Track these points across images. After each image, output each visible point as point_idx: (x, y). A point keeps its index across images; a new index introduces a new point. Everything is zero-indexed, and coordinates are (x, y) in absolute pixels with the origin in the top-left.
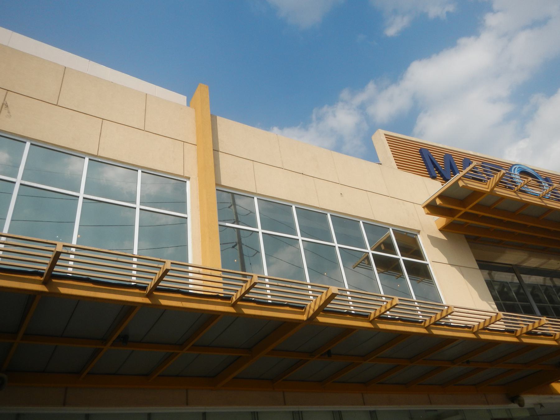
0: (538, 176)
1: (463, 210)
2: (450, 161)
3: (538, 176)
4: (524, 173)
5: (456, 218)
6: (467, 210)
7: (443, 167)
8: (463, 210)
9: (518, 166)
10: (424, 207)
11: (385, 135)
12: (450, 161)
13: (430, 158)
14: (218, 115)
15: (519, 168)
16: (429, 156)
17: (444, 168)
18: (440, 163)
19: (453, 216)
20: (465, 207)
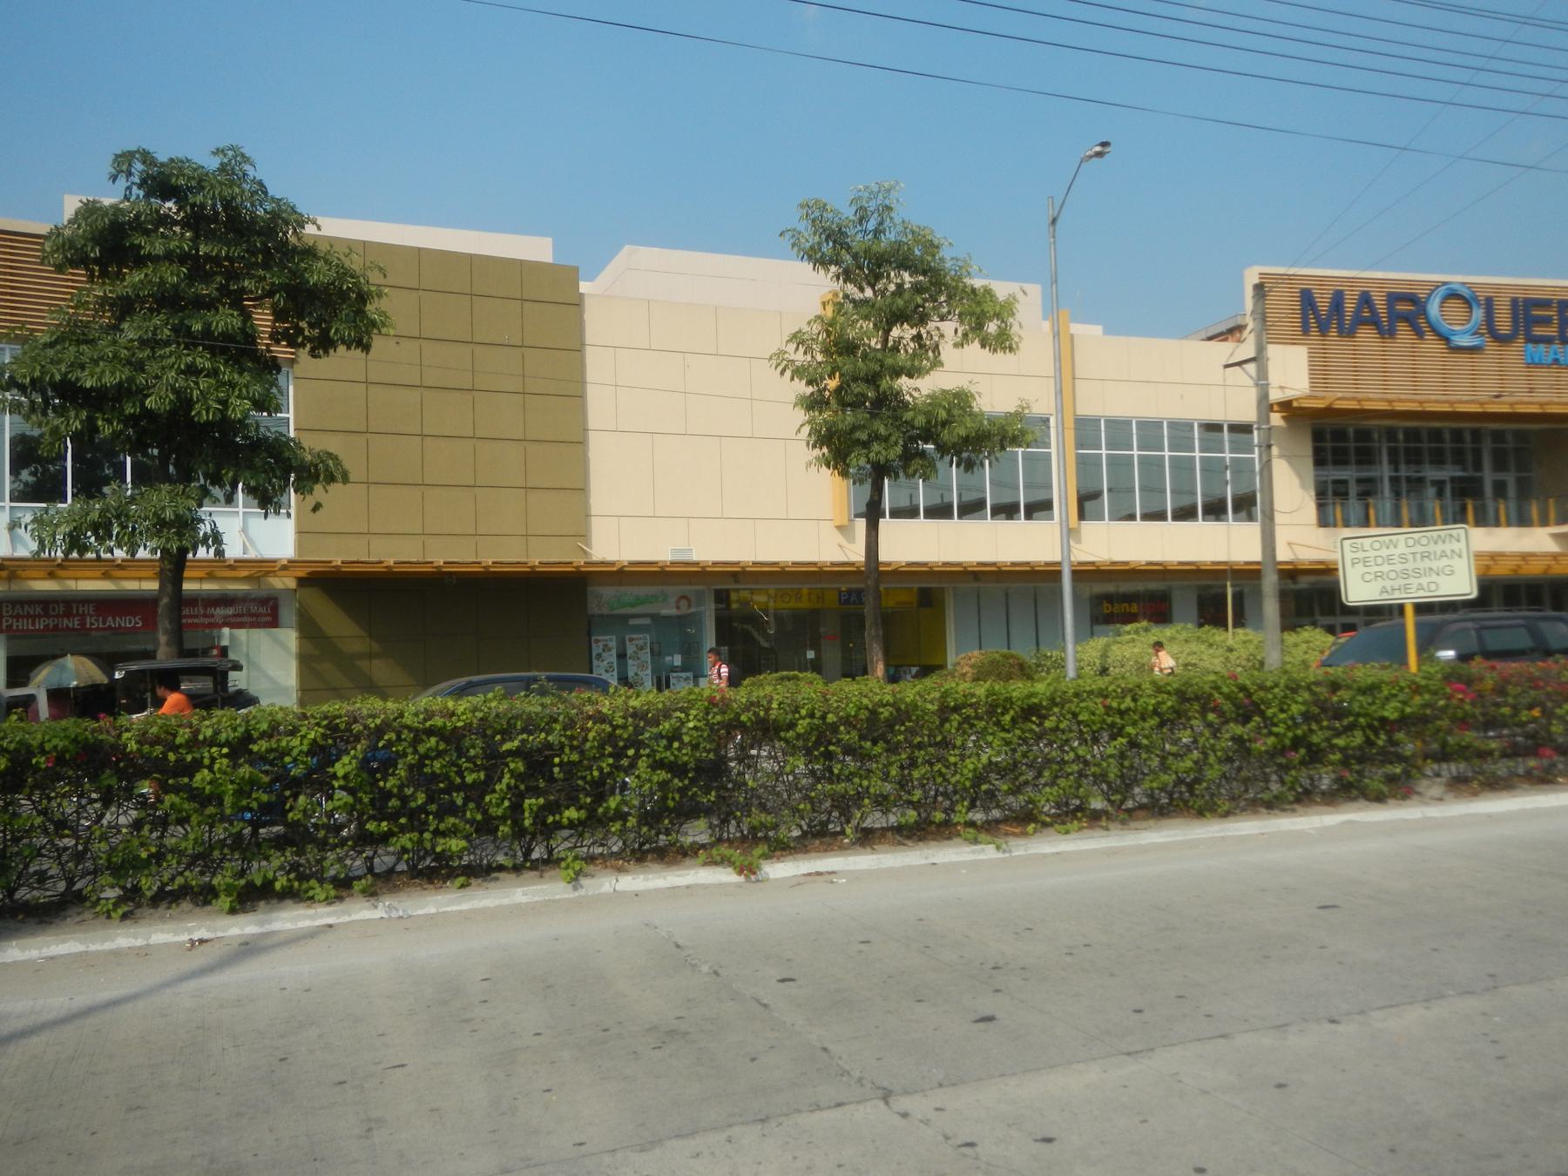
4: (1453, 295)
9: (1445, 287)
18: (1323, 304)
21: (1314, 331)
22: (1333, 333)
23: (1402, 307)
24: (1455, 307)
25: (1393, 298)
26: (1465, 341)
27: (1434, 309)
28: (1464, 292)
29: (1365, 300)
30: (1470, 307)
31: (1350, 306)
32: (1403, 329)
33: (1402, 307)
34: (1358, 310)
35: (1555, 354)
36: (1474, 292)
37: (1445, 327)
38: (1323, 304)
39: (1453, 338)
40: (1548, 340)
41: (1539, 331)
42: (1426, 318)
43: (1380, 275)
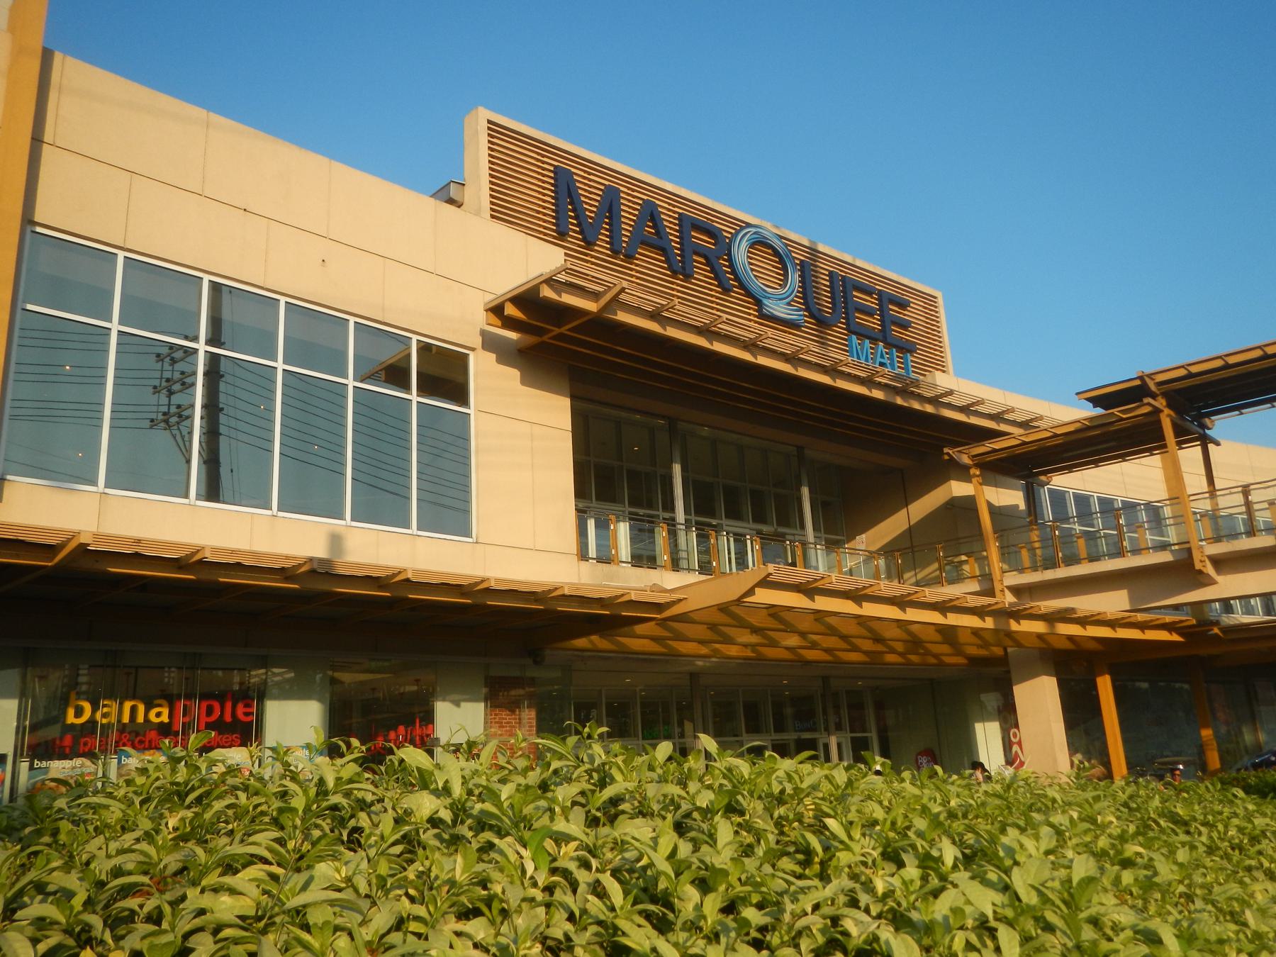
0: (787, 256)
1: (557, 331)
2: (611, 202)
3: (787, 256)
4: (760, 243)
5: (545, 338)
6: (564, 330)
7: (591, 218)
8: (557, 331)
9: (754, 230)
10: (487, 311)
11: (489, 122)
12: (611, 202)
13: (569, 189)
14: (66, 52)
15: (755, 233)
16: (569, 189)
17: (591, 221)
18: (591, 202)
19: (541, 337)
20: (559, 327)
21: (574, 238)
22: (602, 246)
23: (700, 239)
24: (766, 265)
25: (688, 224)
26: (779, 309)
27: (741, 253)
28: (777, 244)
29: (650, 214)
30: (785, 269)
31: (628, 216)
32: (701, 272)
33: (700, 239)
34: (638, 225)
35: (882, 357)
36: (787, 245)
37: (756, 284)
38: (591, 202)
39: (765, 301)
40: (874, 340)
41: (861, 319)
42: (730, 260)
43: (669, 186)
